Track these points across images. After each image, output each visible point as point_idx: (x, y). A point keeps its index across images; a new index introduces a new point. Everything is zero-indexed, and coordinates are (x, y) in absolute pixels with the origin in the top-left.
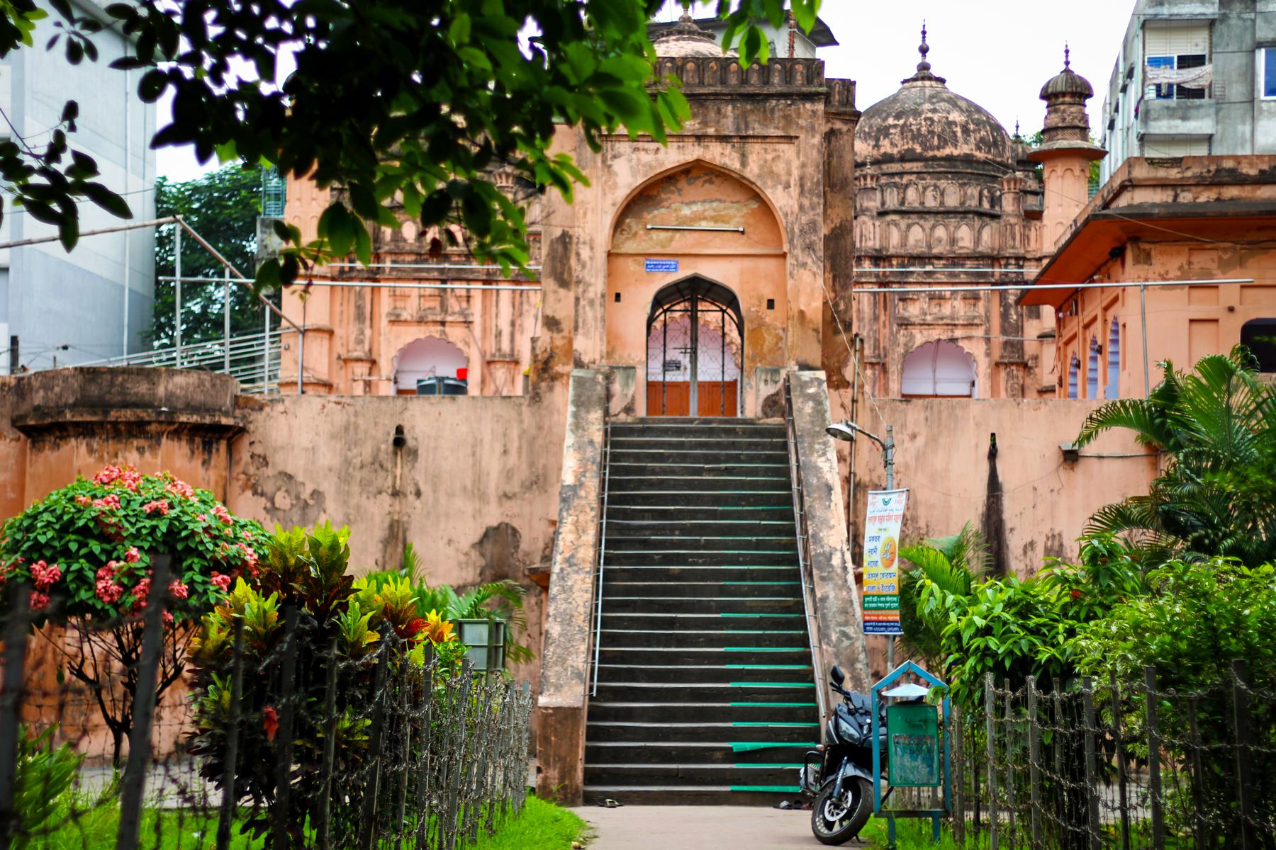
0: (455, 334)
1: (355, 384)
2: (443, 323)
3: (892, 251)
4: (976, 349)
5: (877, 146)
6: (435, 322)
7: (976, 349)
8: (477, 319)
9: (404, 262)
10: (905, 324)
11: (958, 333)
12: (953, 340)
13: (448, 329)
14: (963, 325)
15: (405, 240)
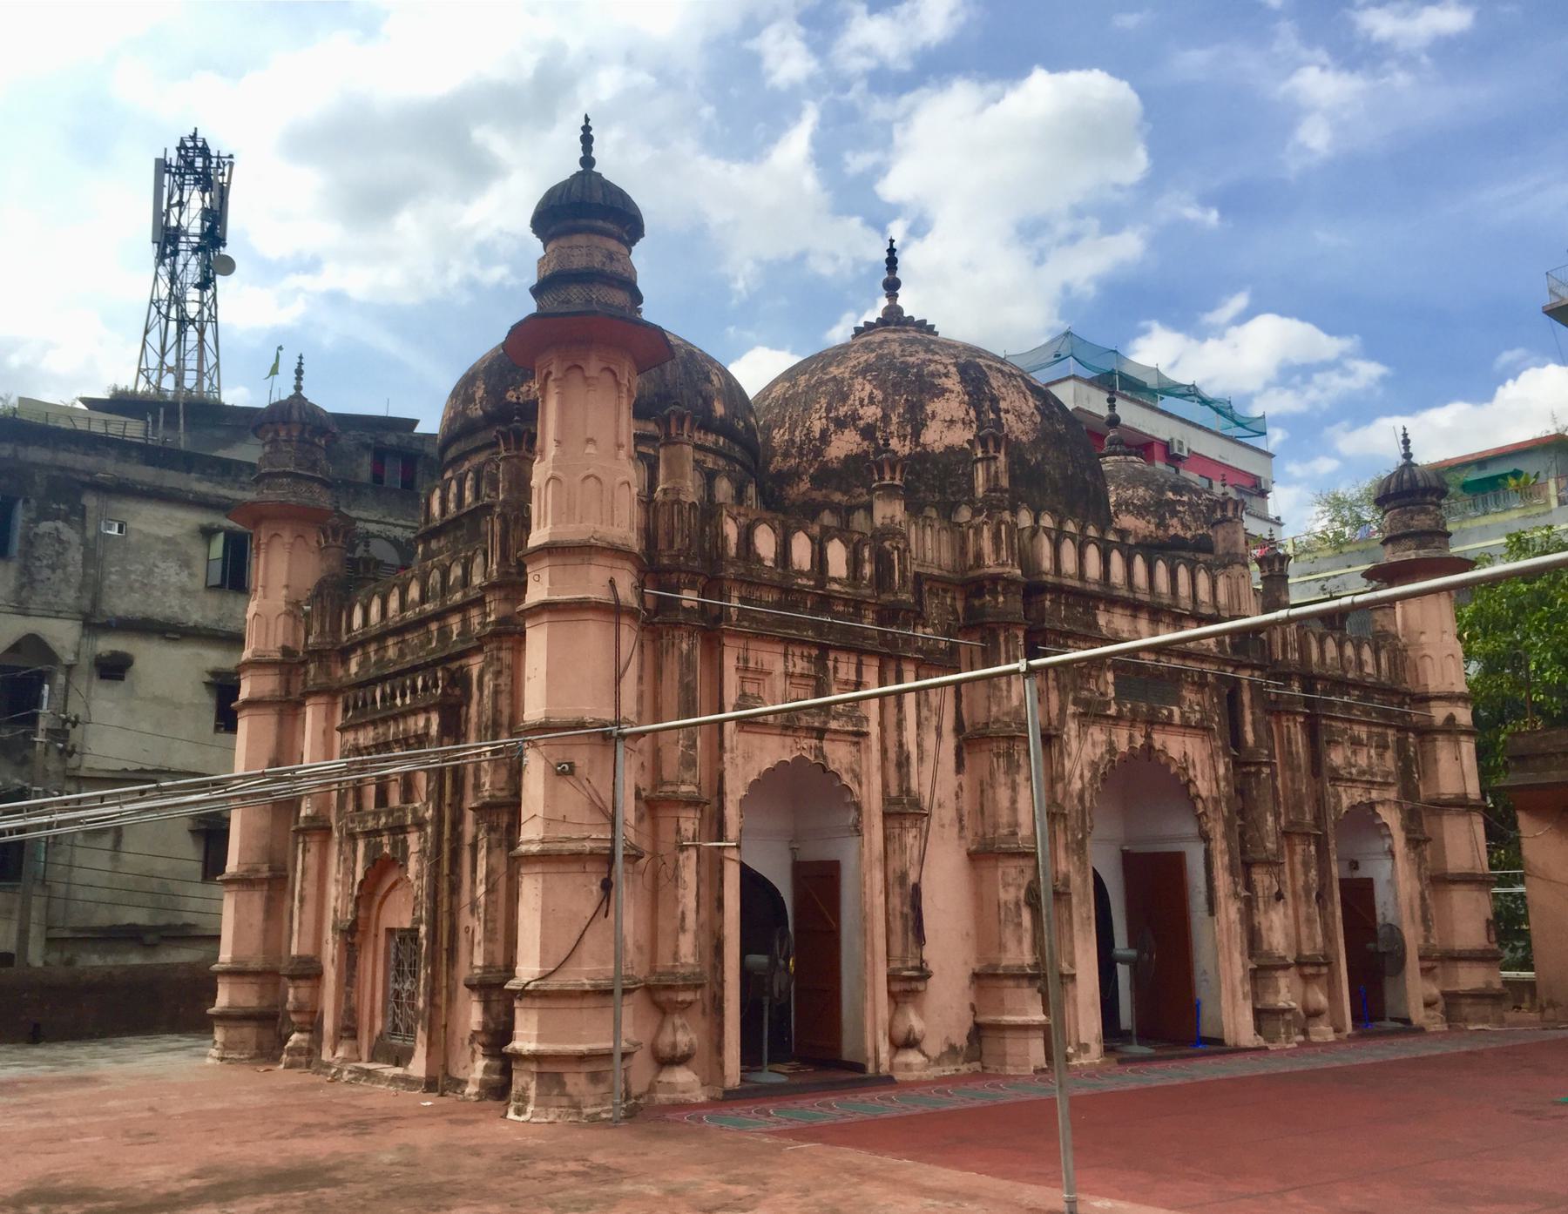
0: (839, 754)
1: (681, 857)
2: (821, 733)
3: (1316, 670)
4: (1391, 817)
5: (1162, 524)
6: (810, 729)
7: (1391, 817)
8: (873, 728)
9: (760, 602)
10: (1336, 778)
11: (1374, 795)
12: (1372, 805)
13: (827, 746)
14: (1381, 784)
15: (760, 560)
